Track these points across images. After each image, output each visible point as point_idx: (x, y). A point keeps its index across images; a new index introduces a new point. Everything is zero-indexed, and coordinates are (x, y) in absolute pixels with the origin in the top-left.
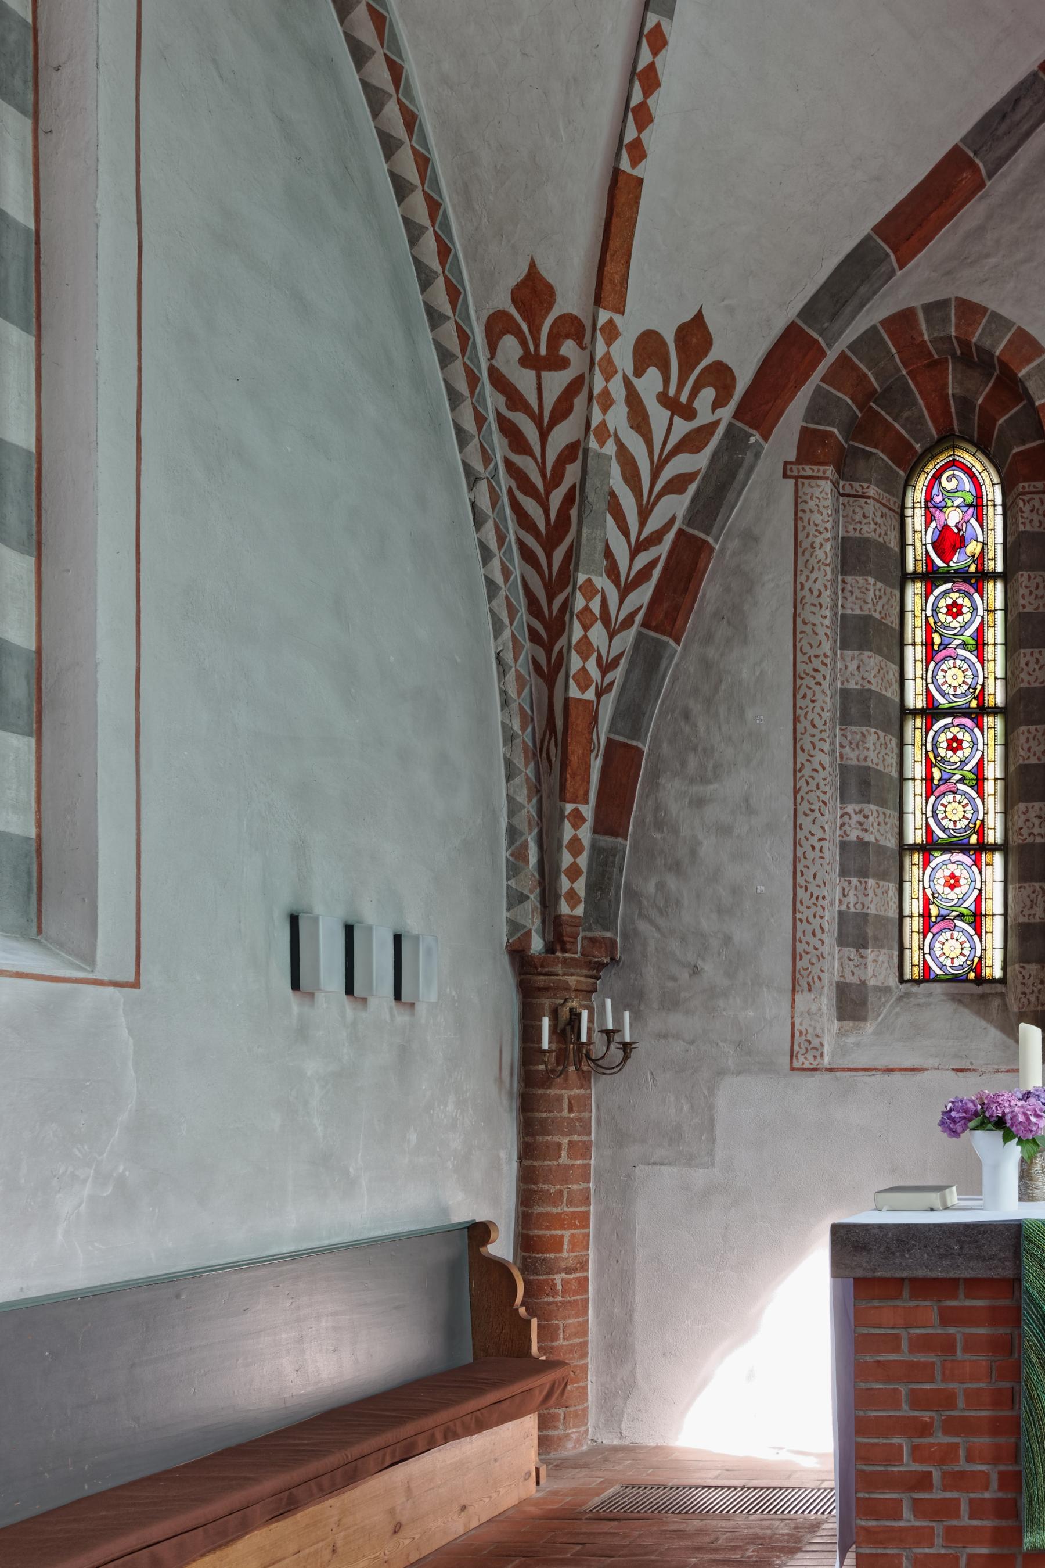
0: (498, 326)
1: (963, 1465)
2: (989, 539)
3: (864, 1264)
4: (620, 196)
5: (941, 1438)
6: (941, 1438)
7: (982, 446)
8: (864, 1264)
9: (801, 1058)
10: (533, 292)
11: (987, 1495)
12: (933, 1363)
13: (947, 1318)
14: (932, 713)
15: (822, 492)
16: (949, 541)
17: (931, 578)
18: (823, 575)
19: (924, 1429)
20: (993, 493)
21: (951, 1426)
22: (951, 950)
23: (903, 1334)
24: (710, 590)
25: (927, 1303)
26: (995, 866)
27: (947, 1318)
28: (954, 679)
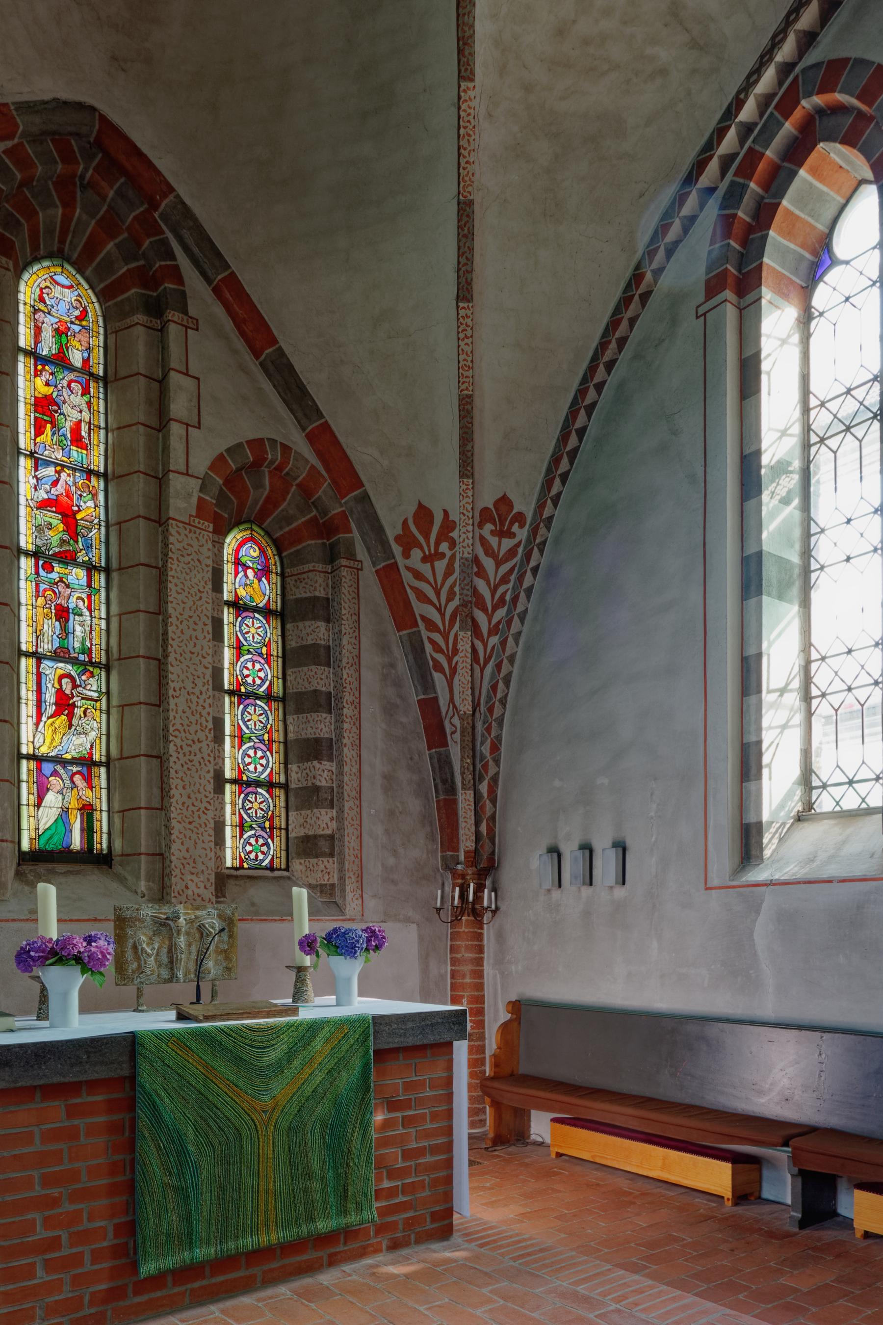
1: (86, 1225)
3: (7, 1078)
5: (67, 1207)
6: (67, 1207)
8: (7, 1078)
11: (105, 1244)
12: (61, 1150)
13: (71, 1112)
19: (55, 1202)
21: (74, 1197)
23: (36, 1130)
25: (56, 1103)
27: (71, 1112)
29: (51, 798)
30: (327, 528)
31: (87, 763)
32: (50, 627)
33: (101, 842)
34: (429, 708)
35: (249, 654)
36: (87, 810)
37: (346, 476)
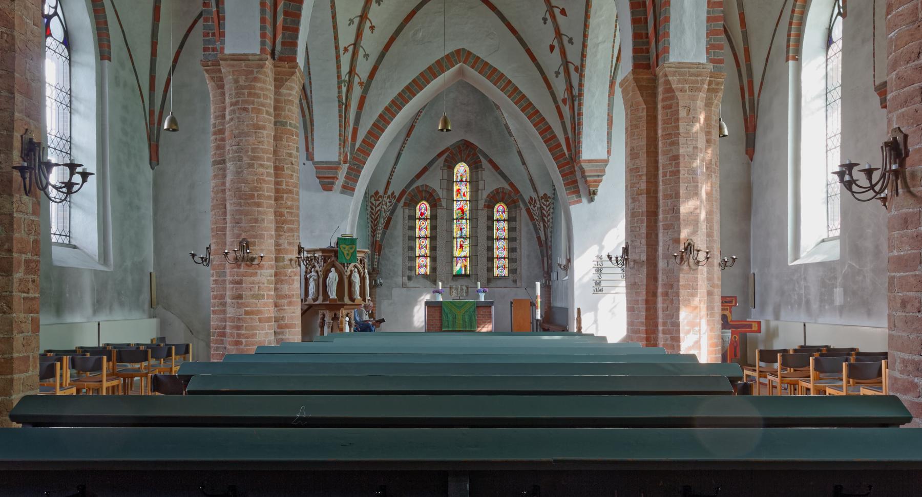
0: (372, 196)
2: (428, 213)
4: (388, 183)
7: (427, 201)
9: (404, 286)
10: (377, 193)
14: (420, 238)
15: (407, 210)
16: (422, 214)
17: (420, 219)
18: (406, 222)
20: (428, 208)
22: (422, 271)
24: (392, 223)
26: (428, 259)
28: (423, 233)
29: (459, 265)
30: (514, 202)
31: (465, 257)
32: (459, 232)
33: (468, 272)
34: (539, 238)
35: (501, 229)
36: (465, 266)
37: (517, 191)
